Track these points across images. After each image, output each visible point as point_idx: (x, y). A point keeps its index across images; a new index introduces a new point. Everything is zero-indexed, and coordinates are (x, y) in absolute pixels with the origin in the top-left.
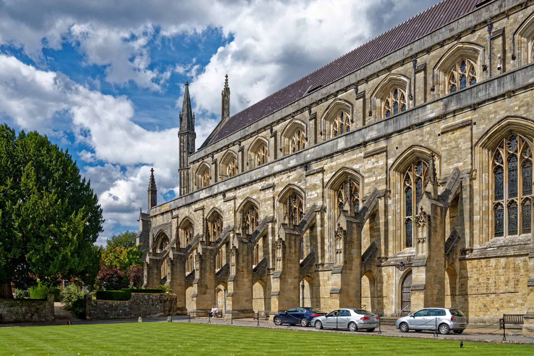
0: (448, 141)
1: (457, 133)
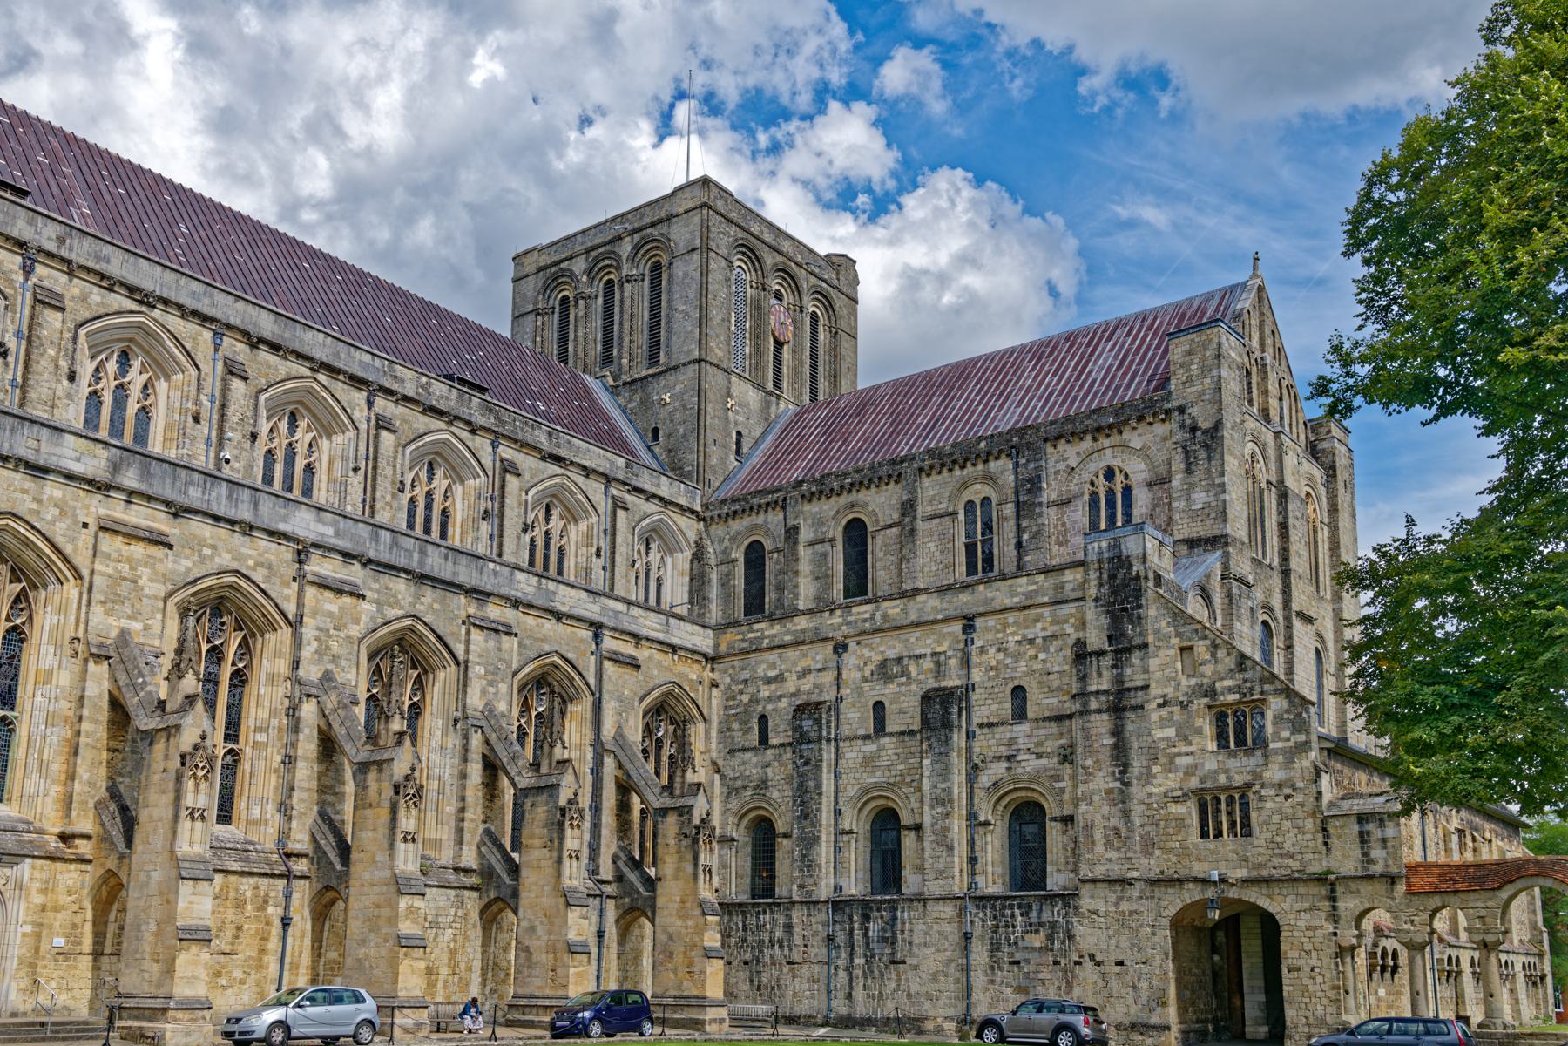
0: (114, 555)
1: (138, 549)
